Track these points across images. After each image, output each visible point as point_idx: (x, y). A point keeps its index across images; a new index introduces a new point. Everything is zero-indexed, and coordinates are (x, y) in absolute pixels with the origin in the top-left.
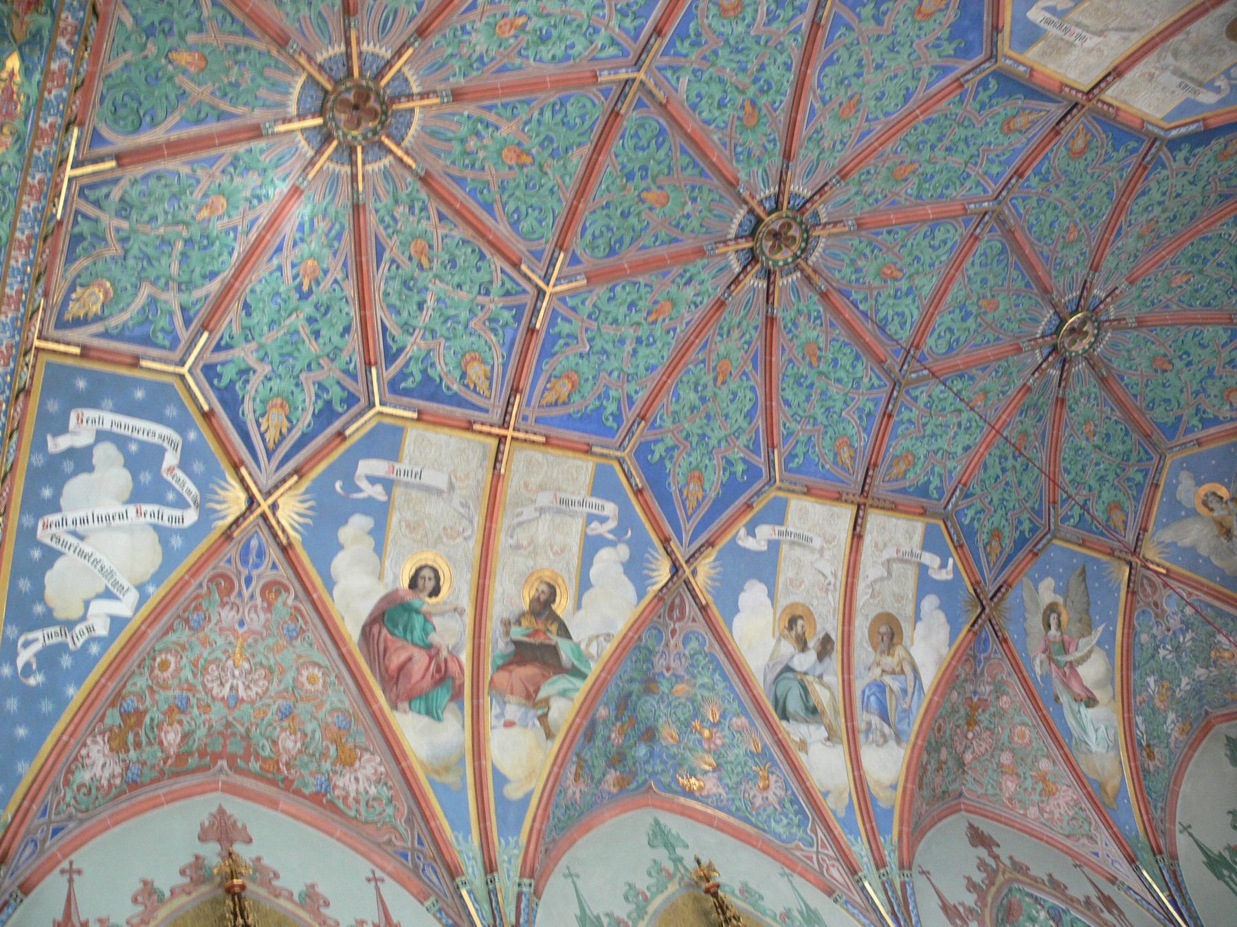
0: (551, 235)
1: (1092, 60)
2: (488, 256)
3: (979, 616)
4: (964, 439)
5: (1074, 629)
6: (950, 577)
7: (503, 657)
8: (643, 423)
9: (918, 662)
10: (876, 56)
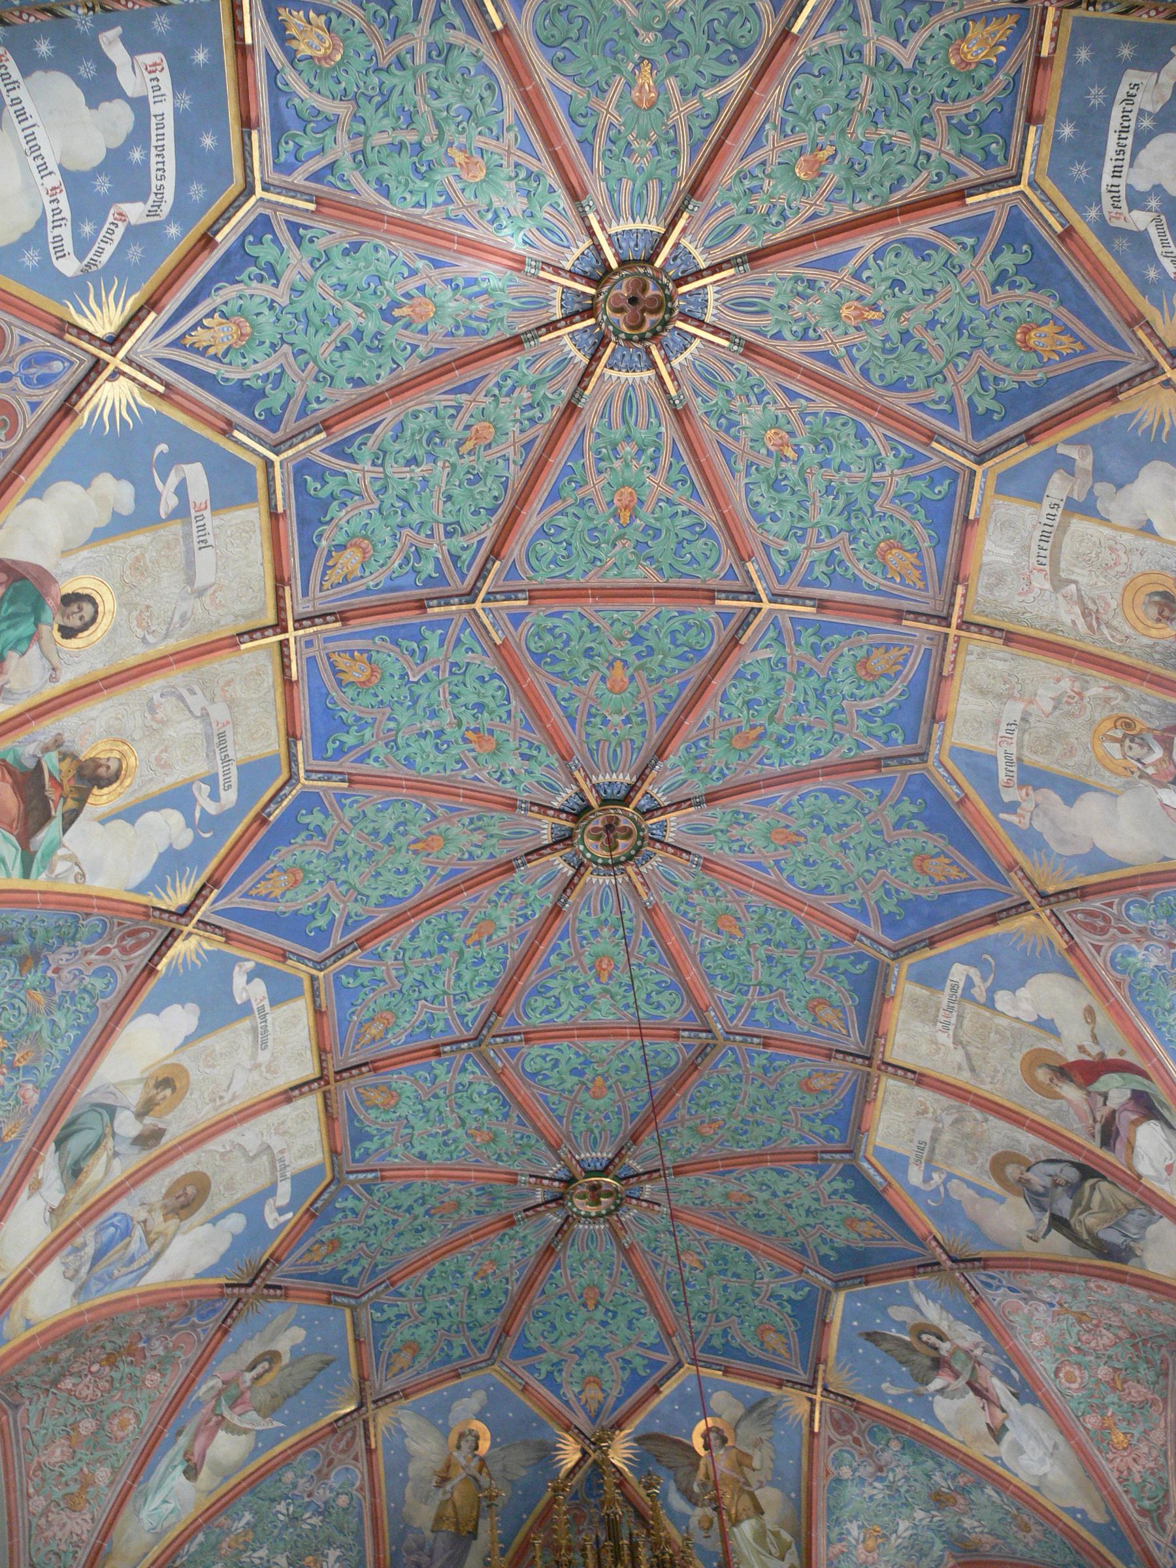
0: (541, 580)
1: (924, 1048)
2: (494, 519)
3: (240, 1286)
4: (431, 1147)
5: (261, 1396)
6: (271, 1226)
7: (17, 760)
8: (346, 785)
9: (169, 1253)
10: (857, 838)
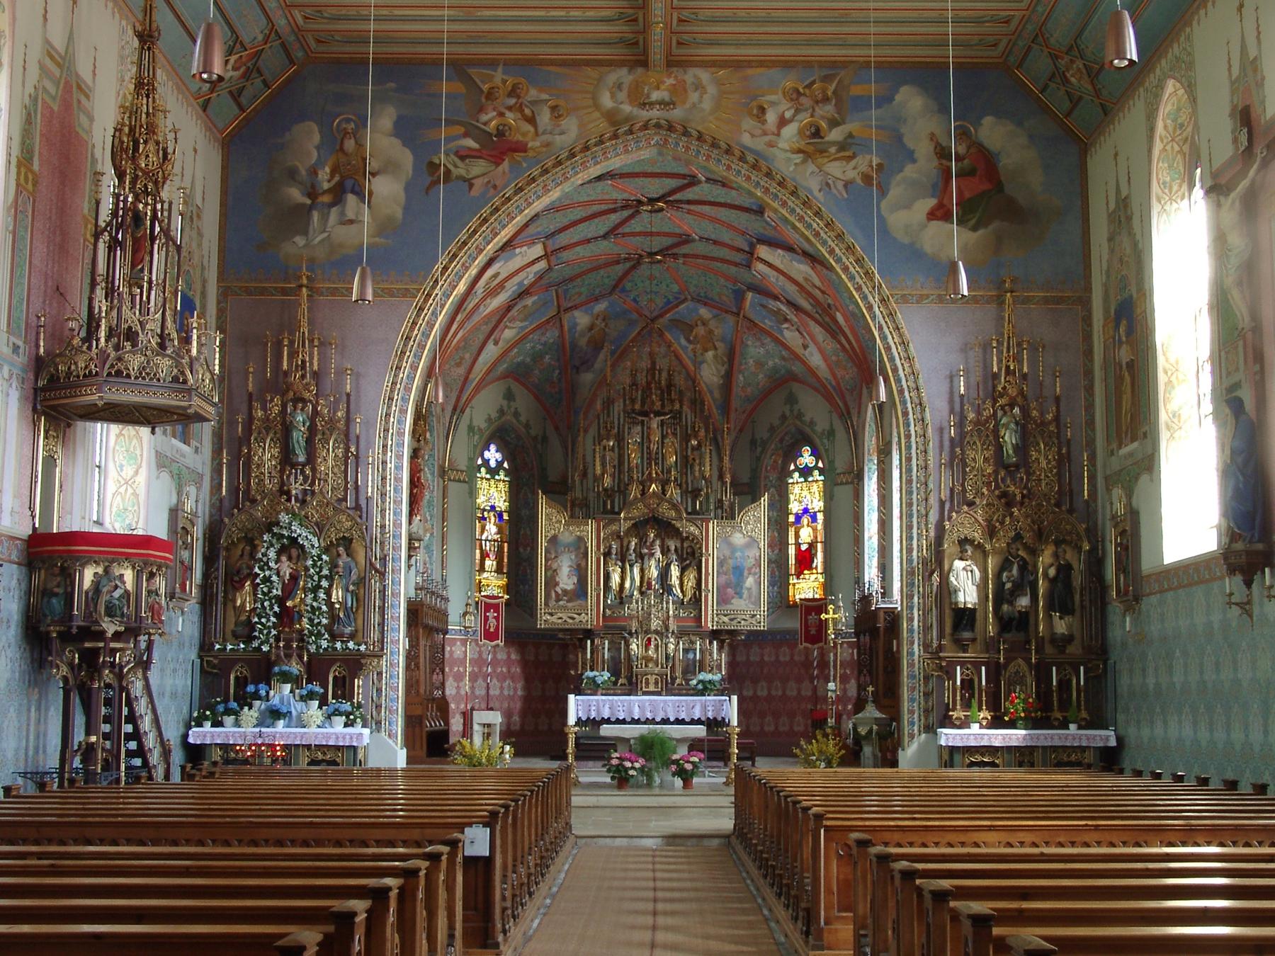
5: (522, 316)
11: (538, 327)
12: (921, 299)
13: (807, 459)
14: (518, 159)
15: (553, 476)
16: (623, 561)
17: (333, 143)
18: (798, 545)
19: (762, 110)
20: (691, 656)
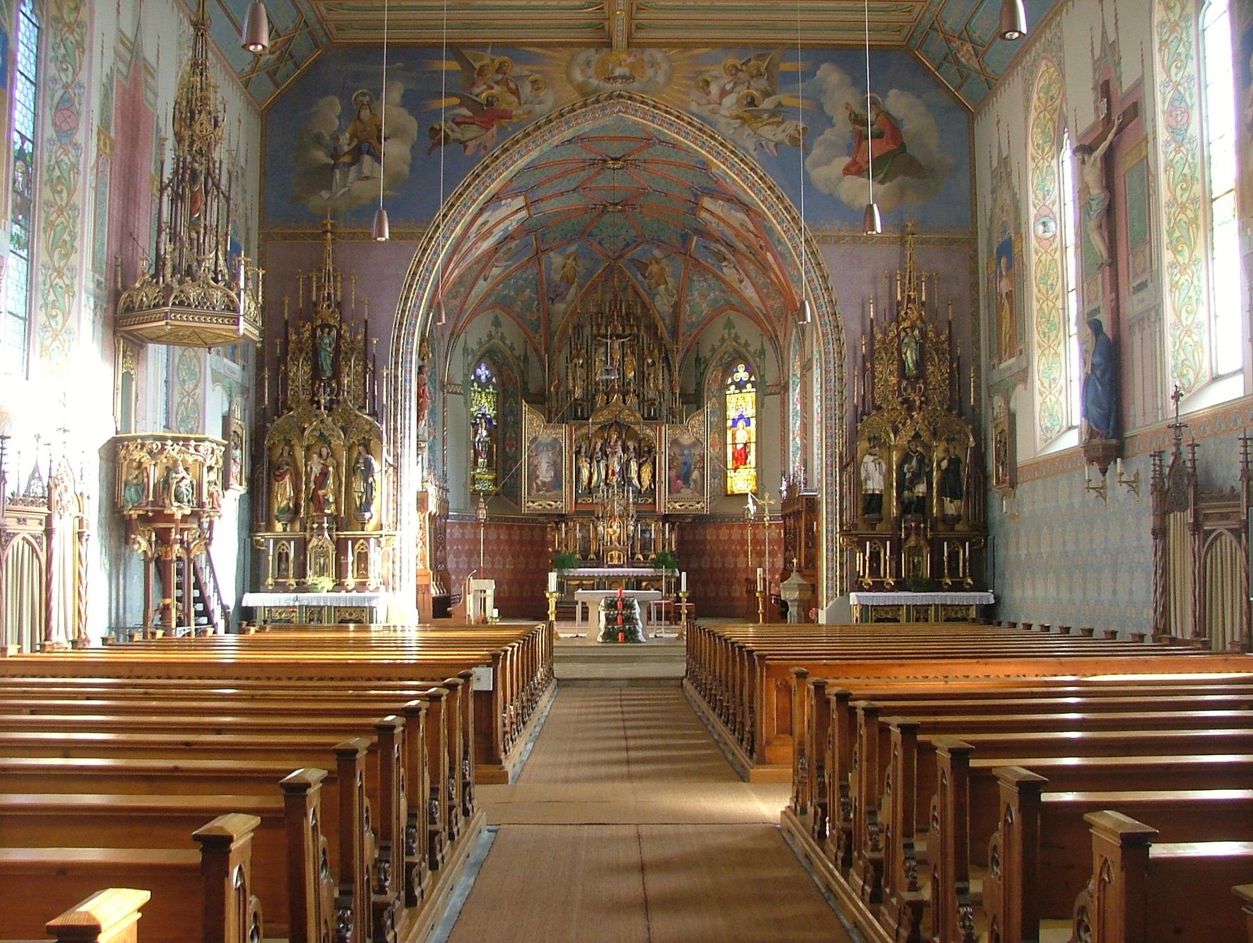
11: (522, 266)
12: (838, 239)
13: (741, 374)
14: (505, 124)
15: (532, 388)
16: (591, 459)
17: (351, 113)
18: (735, 444)
19: (707, 83)
20: (647, 535)
